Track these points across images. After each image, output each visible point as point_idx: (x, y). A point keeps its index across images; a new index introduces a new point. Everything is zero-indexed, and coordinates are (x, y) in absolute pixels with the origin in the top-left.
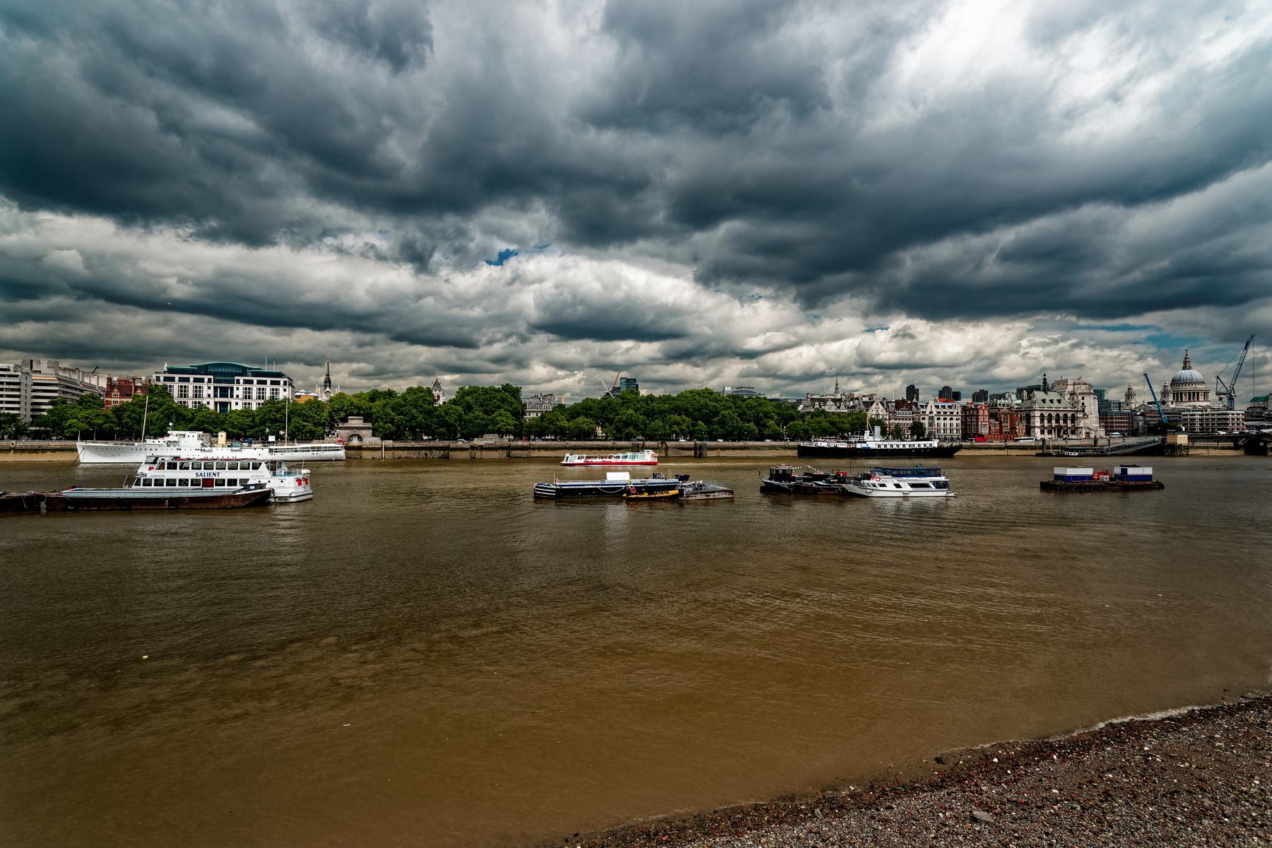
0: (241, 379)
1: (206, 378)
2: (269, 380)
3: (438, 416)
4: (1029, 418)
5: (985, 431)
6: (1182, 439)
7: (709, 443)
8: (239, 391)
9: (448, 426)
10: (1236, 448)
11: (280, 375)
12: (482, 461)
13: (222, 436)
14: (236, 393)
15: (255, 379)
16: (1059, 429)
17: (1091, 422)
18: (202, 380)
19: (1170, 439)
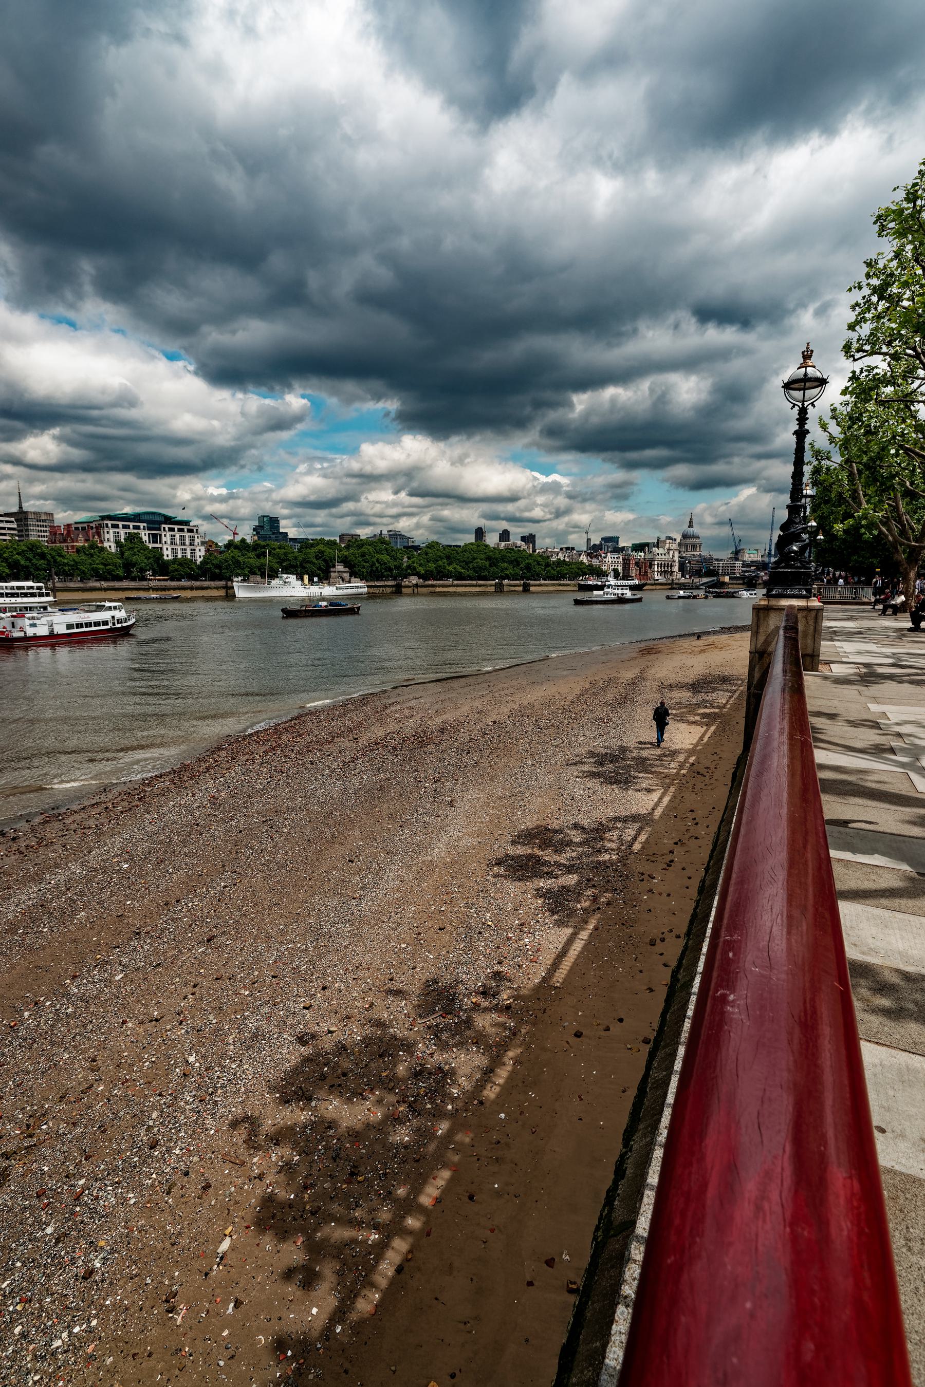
0: (167, 527)
1: (142, 525)
2: (186, 528)
3: (385, 564)
4: (651, 566)
5: (633, 574)
6: (727, 579)
7: (532, 582)
8: (166, 538)
9: (390, 570)
10: (743, 584)
11: (187, 523)
12: (418, 594)
13: (306, 577)
14: (164, 539)
15: (176, 527)
16: (665, 572)
17: (676, 569)
18: (138, 528)
19: (722, 579)
